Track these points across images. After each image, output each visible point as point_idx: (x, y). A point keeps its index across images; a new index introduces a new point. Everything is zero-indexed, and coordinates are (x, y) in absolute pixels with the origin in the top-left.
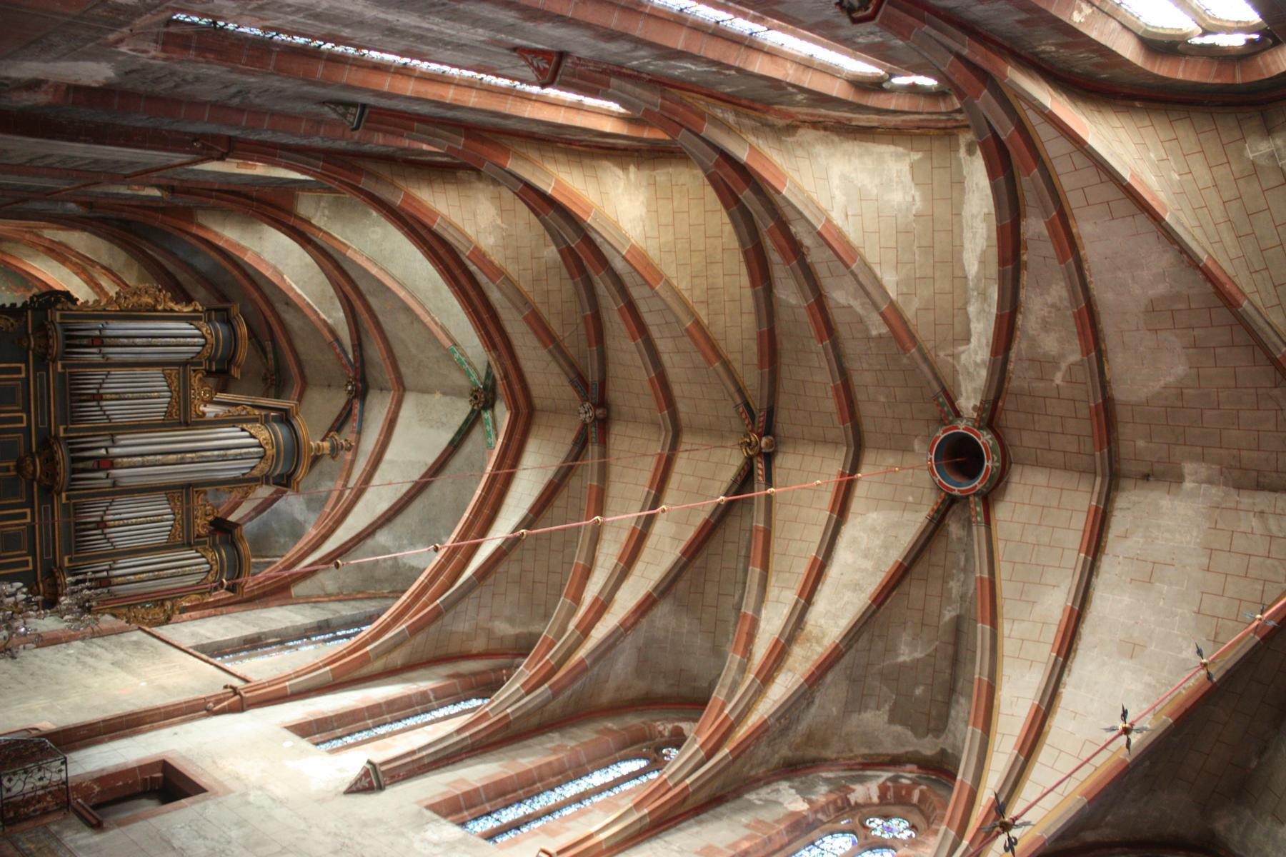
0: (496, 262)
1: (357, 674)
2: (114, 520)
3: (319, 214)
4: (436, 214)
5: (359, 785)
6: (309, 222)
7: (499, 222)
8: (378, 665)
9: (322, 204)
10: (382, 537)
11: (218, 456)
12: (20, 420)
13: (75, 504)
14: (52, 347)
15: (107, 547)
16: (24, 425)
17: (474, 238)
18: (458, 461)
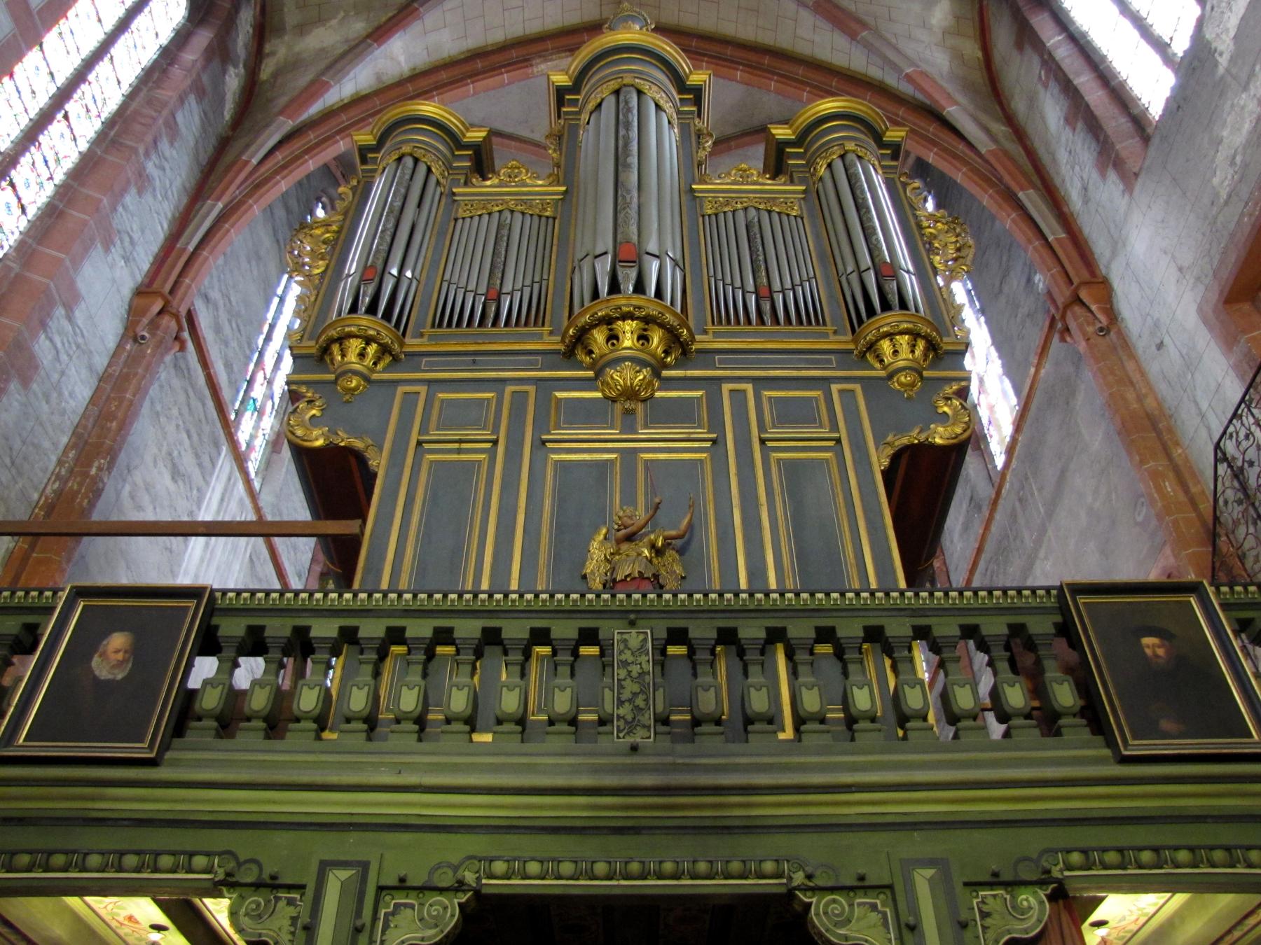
1: (1029, 167)
7: (334, 22)
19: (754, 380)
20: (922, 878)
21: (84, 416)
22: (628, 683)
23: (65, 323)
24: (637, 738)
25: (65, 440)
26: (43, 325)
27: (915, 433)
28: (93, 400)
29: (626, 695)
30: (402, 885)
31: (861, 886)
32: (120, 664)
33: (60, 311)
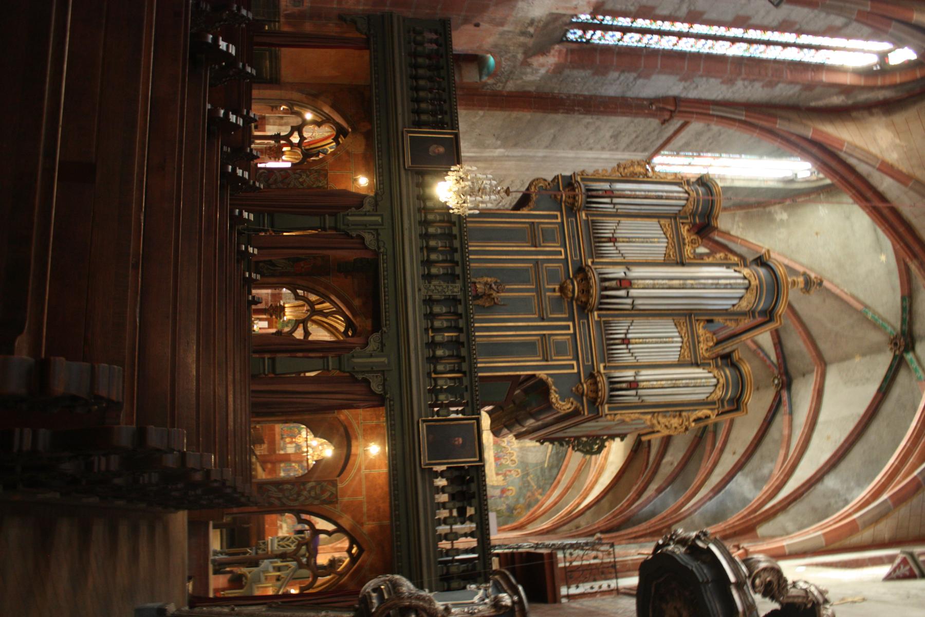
0: (905, 170)
2: (636, 338)
3: (735, 227)
4: (844, 141)
5: (898, 573)
6: (726, 234)
7: (898, 141)
8: (866, 535)
9: (737, 219)
10: (831, 482)
11: (712, 284)
12: (560, 253)
13: (605, 322)
14: (577, 201)
15: (630, 360)
16: (563, 257)
17: (879, 155)
18: (889, 406)
19: (575, 334)
20: (384, 360)
21: (601, 97)
22: (441, 288)
23: (631, 78)
24: (423, 290)
25: (586, 93)
26: (623, 71)
27: (553, 387)
28: (611, 98)
29: (437, 288)
30: (378, 235)
31: (383, 345)
32: (434, 152)
33: (635, 75)
